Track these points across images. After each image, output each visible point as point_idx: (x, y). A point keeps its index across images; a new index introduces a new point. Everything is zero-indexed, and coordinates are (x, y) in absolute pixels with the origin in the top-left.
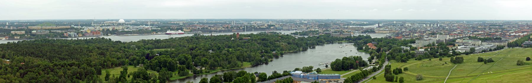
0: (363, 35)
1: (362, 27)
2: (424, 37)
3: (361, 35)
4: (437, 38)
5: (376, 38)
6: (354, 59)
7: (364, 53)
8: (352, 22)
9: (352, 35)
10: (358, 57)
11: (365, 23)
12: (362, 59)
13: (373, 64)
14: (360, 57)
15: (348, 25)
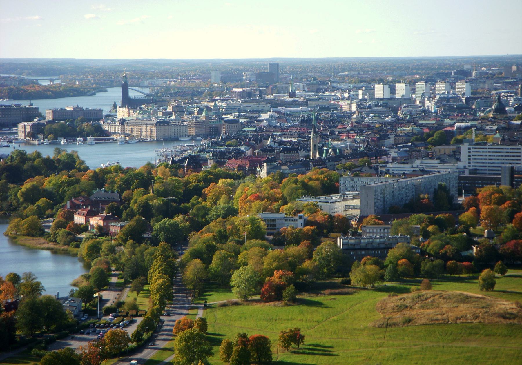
1: (25, 104)
4: (461, 165)
11: (45, 83)
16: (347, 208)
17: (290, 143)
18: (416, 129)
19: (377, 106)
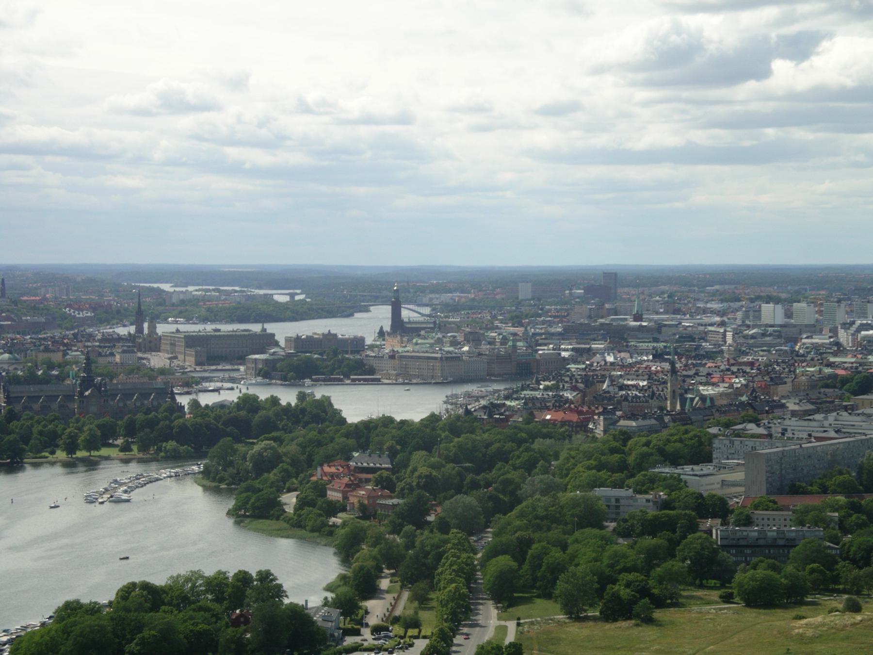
0: (274, 401)
1: (256, 328)
2: (778, 412)
3: (255, 398)
5: (387, 421)
6: (218, 600)
7: (286, 544)
8: (167, 287)
9: (184, 401)
10: (243, 578)
11: (281, 297)
12: (279, 592)
13: (376, 630)
14: (266, 577)
15: (139, 317)
16: (724, 483)
17: (636, 387)
18: (828, 371)
19: (764, 335)
